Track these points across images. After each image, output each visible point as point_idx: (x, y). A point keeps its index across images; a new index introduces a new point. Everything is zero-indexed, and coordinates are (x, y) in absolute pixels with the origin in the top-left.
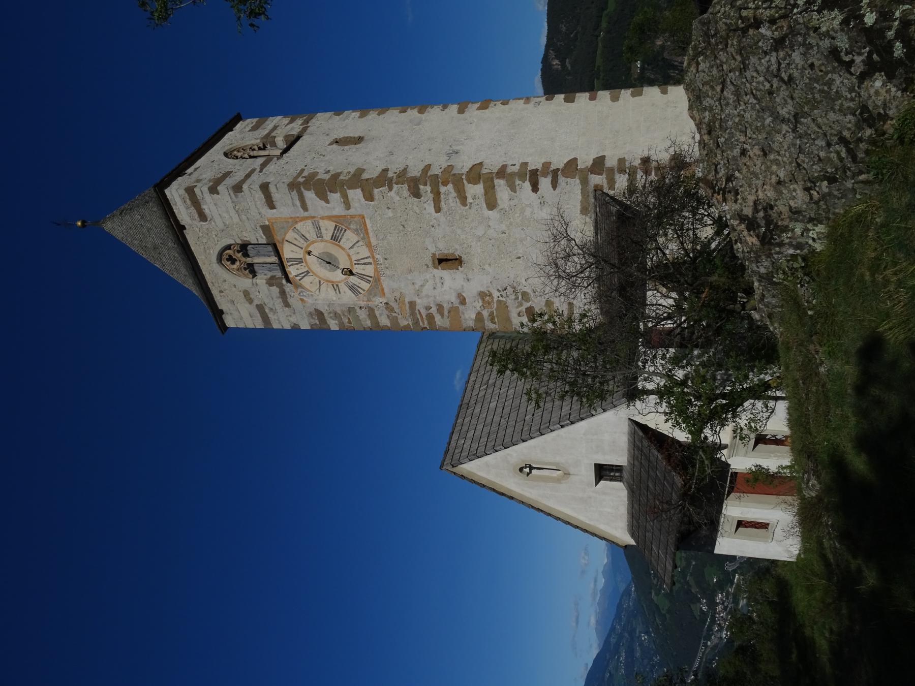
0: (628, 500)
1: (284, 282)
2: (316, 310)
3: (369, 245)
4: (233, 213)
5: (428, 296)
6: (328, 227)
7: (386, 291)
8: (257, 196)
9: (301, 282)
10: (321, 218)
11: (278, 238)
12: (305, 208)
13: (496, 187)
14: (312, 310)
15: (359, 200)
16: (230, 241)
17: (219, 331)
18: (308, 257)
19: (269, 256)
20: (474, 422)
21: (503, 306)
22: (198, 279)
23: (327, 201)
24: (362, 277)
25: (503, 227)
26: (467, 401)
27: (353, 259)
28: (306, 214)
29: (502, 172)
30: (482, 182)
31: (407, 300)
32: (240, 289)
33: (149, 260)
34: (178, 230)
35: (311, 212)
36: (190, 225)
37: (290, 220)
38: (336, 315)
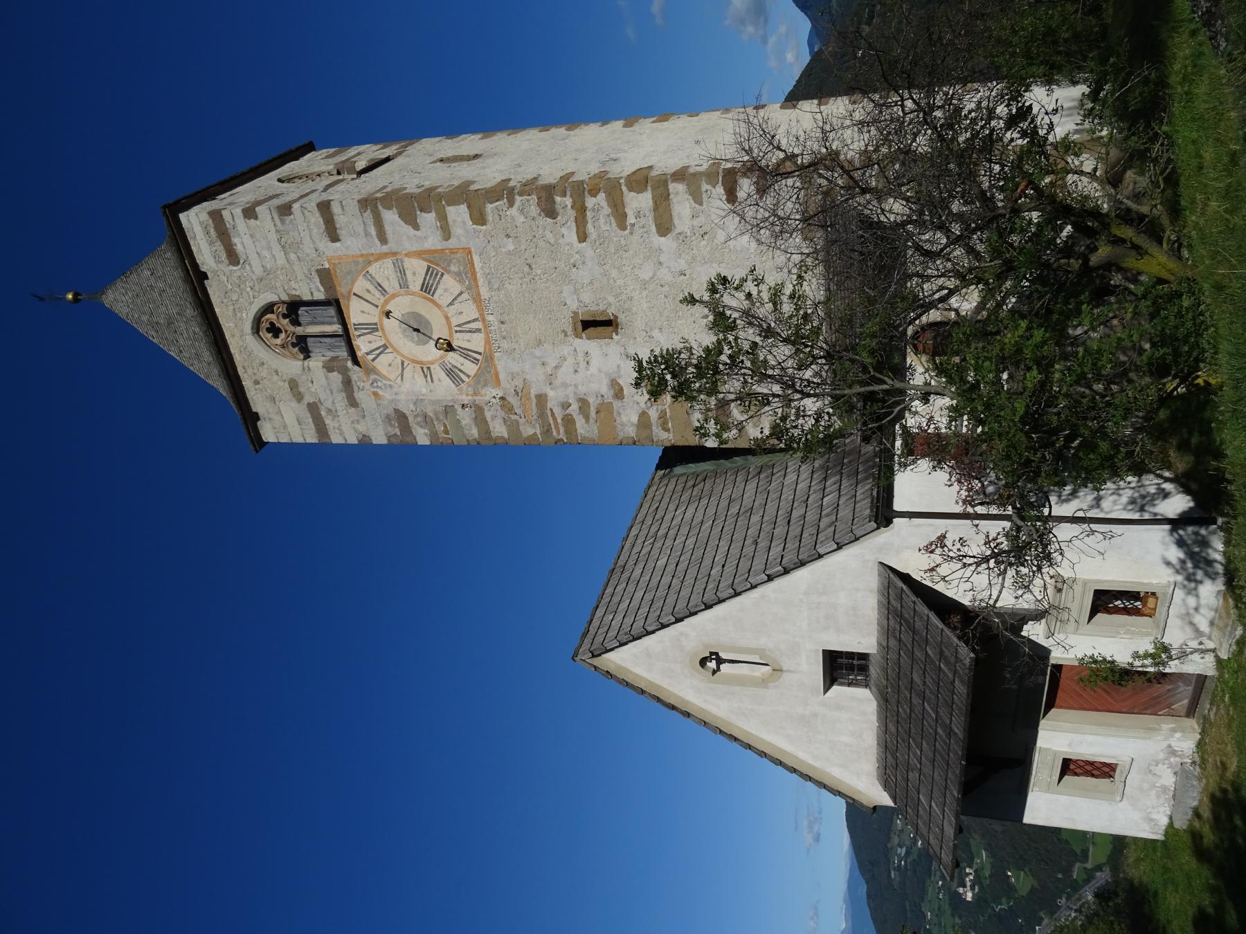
0: (879, 719)
1: (349, 364)
2: (397, 411)
3: (477, 299)
4: (276, 249)
5: (565, 385)
6: (416, 269)
7: (502, 376)
8: (313, 220)
9: (375, 363)
10: (406, 255)
11: (342, 290)
12: (383, 239)
13: (671, 197)
14: (391, 411)
15: (464, 223)
16: (273, 298)
17: (251, 447)
18: (385, 320)
19: (330, 323)
20: (631, 588)
22: (223, 360)
23: (416, 227)
24: (466, 353)
25: (682, 264)
26: (623, 563)
27: (454, 324)
28: (385, 249)
29: (681, 175)
30: (649, 188)
31: (533, 393)
32: (284, 378)
33: (161, 346)
34: (196, 279)
35: (391, 246)
36: (215, 272)
37: (360, 260)
38: (426, 420)
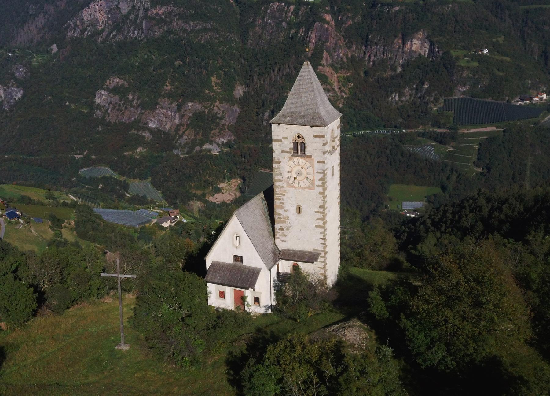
3: (305, 188)
6: (311, 177)
12: (317, 172)
23: (319, 180)
24: (294, 182)
35: (316, 174)
38: (279, 168)
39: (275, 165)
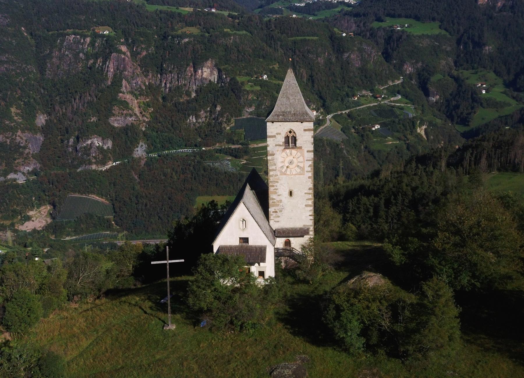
3: (296, 174)
6: (301, 165)
12: (307, 160)
21: (278, 205)
24: (286, 170)
35: (306, 162)
38: (273, 160)
39: (269, 158)
